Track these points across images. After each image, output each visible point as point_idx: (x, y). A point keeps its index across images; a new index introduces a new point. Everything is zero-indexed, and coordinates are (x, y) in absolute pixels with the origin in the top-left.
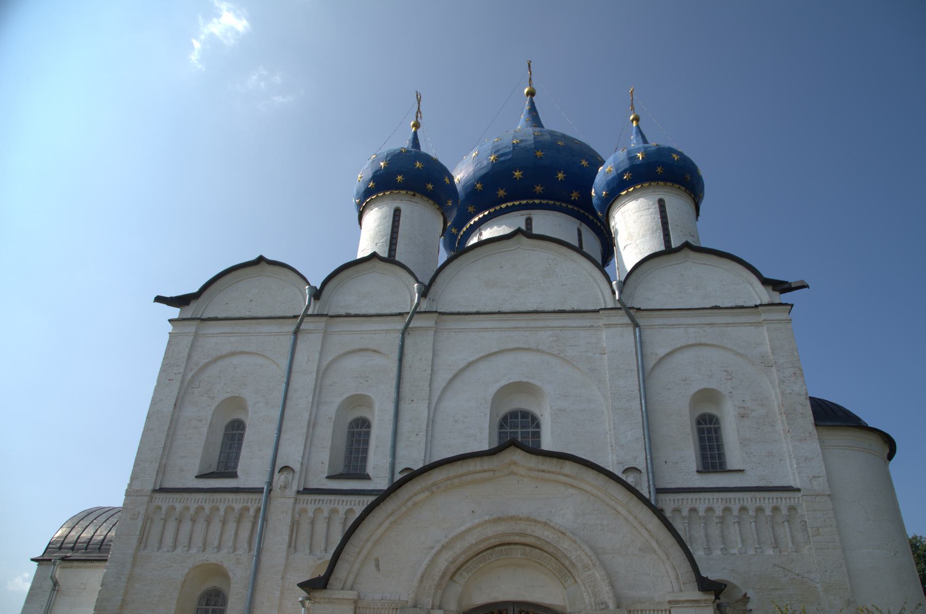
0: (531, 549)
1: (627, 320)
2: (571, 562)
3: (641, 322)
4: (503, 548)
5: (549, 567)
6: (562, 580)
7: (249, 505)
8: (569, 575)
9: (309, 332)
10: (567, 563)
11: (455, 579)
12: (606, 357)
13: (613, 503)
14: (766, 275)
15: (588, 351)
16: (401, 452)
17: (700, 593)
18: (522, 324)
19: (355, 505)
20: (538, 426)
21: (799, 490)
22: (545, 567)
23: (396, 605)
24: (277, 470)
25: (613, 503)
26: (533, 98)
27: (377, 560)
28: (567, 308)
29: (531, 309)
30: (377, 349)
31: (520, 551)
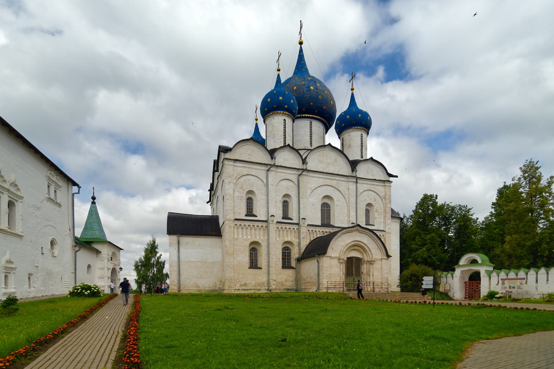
1: (355, 181)
3: (358, 181)
7: (263, 225)
10: (365, 250)
14: (389, 172)
15: (344, 188)
16: (301, 213)
18: (329, 177)
20: (330, 208)
24: (270, 216)
27: (332, 248)
28: (340, 174)
29: (331, 172)
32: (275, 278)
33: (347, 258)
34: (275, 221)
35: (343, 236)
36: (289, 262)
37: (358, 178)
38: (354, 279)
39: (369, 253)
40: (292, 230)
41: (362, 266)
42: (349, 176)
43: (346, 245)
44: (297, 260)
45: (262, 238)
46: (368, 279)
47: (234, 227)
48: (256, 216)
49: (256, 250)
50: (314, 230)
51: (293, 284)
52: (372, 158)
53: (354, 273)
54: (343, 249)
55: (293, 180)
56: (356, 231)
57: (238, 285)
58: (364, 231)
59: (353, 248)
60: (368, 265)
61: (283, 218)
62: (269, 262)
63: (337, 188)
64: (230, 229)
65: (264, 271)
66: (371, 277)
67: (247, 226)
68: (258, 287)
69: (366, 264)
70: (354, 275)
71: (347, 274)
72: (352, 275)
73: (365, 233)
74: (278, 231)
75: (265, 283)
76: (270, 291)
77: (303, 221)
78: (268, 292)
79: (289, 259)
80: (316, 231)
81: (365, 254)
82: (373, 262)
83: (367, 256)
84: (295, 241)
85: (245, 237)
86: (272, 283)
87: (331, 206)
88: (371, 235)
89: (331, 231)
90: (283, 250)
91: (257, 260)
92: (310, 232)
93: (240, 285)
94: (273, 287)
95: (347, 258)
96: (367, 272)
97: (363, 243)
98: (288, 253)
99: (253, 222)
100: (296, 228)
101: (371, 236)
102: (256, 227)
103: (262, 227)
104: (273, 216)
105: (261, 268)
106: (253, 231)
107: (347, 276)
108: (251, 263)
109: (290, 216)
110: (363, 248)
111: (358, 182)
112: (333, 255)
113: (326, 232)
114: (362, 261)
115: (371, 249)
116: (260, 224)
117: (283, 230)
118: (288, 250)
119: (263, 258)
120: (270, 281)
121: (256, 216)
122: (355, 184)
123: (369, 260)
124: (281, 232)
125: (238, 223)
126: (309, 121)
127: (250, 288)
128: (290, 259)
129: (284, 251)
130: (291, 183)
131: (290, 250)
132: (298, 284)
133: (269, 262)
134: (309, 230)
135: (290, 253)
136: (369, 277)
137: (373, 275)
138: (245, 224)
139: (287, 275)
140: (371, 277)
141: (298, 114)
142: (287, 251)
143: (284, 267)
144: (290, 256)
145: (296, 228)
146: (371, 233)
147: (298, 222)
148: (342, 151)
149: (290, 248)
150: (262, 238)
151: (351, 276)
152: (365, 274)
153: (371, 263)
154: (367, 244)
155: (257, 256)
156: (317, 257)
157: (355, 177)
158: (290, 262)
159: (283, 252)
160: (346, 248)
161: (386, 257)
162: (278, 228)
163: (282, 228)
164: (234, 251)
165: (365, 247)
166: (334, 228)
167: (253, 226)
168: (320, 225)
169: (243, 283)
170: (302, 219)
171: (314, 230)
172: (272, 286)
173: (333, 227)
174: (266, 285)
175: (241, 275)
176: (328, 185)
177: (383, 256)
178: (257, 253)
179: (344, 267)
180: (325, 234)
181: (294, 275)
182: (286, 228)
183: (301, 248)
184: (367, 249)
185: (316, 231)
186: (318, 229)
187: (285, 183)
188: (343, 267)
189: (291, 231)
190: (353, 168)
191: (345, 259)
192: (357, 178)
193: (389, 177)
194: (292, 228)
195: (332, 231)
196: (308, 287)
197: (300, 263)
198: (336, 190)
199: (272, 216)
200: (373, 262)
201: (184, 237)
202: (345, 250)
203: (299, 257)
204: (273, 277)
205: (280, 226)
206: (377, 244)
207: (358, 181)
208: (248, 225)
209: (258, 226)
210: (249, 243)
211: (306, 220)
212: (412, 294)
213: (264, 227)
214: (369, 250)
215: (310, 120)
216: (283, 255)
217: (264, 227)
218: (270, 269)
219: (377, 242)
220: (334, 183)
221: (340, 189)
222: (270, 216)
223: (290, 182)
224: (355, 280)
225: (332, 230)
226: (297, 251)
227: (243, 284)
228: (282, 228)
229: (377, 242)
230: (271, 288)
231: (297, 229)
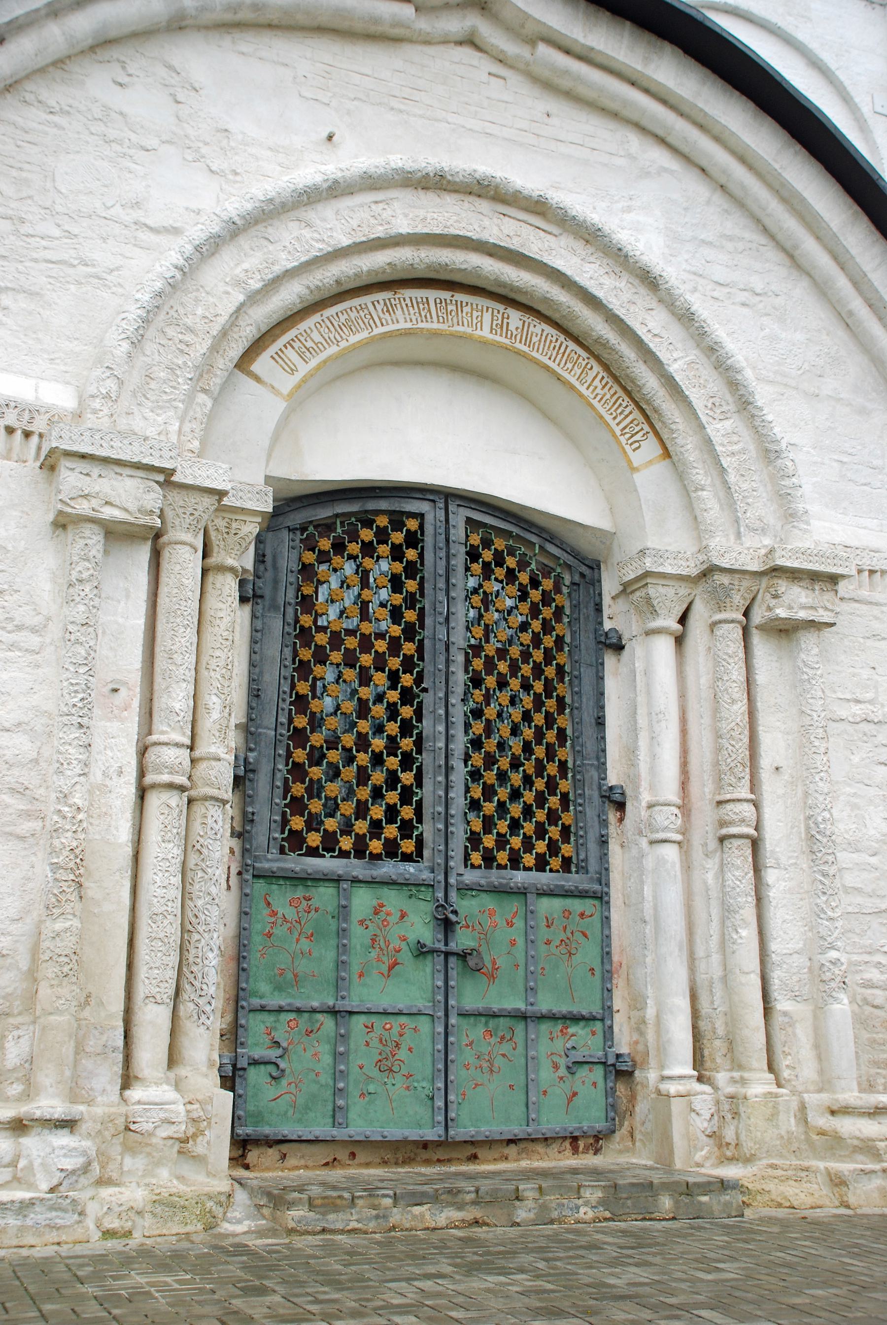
0: (529, 319)
4: (432, 294)
5: (583, 389)
6: (623, 439)
8: (647, 428)
10: (650, 383)
11: (257, 367)
13: (790, 225)
22: (572, 388)
23: (26, 416)
31: (487, 317)
41: (612, 686)
46: (727, 911)
66: (771, 876)
69: (679, 640)
83: (680, 474)
88: (743, 158)
114: (609, 586)
151: (391, 850)
214: (715, 385)
224: (463, 940)
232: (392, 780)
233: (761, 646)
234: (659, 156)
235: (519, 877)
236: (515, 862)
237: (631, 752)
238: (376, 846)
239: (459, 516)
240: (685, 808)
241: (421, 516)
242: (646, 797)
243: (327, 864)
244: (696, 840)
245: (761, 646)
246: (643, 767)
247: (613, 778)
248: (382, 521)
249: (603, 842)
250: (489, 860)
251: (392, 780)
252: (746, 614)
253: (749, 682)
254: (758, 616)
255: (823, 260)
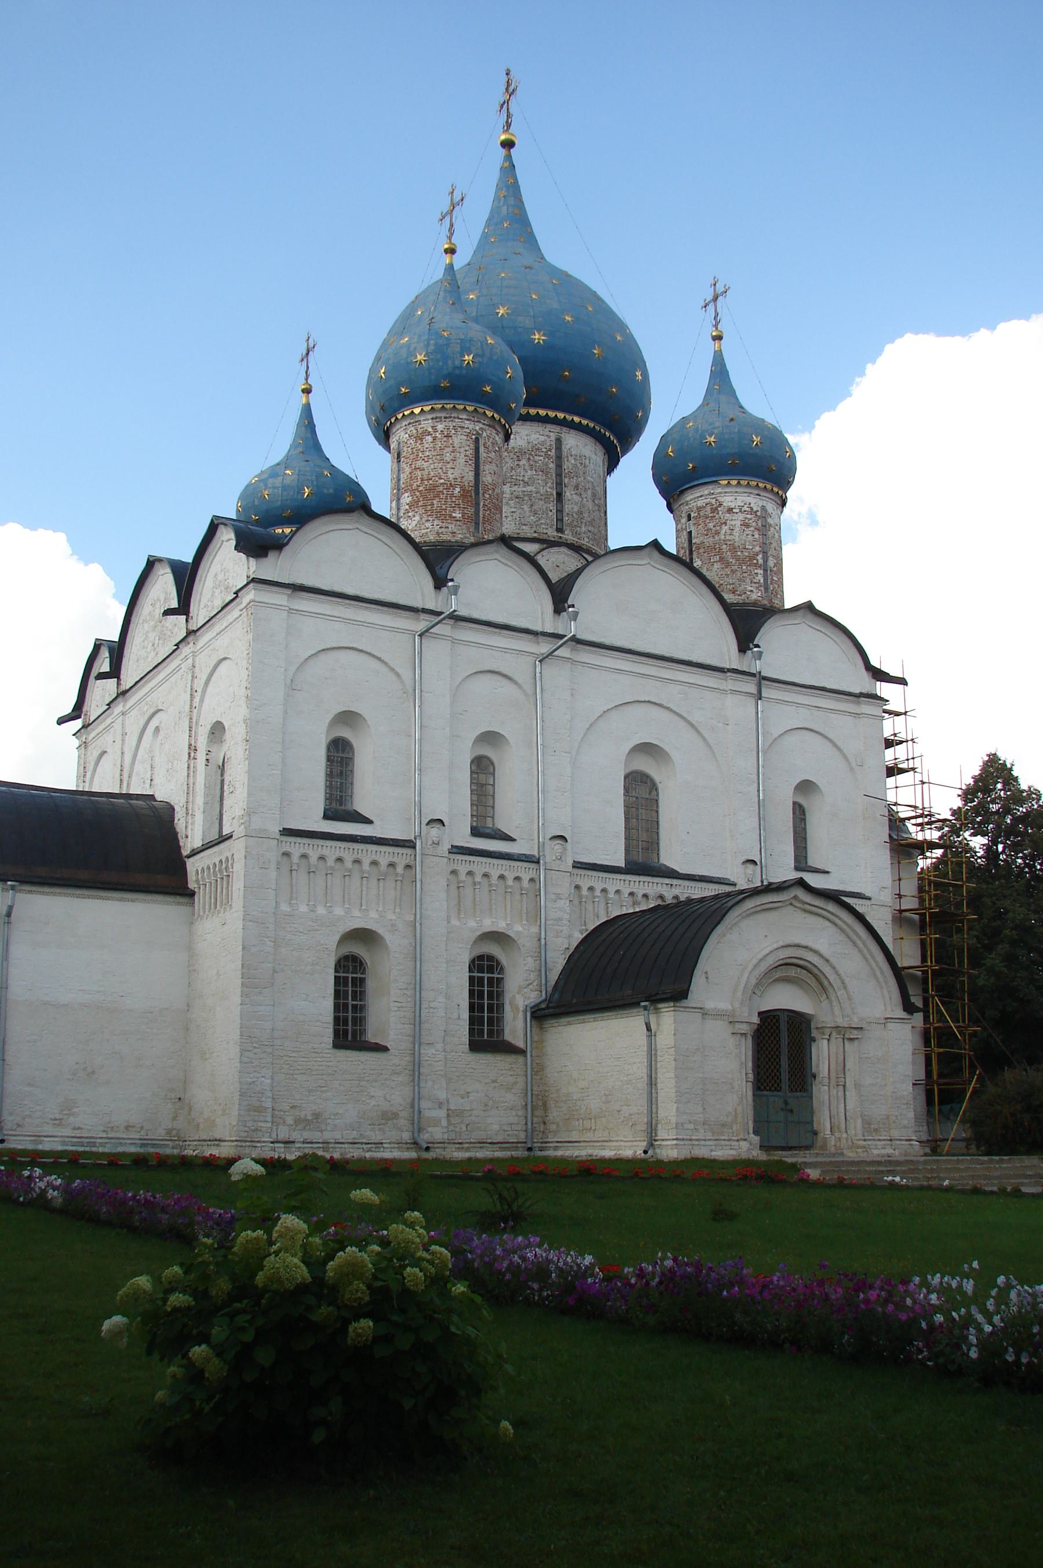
1: (752, 688)
2: (830, 982)
7: (395, 860)
9: (437, 637)
10: (826, 983)
12: (729, 728)
13: (855, 938)
14: (874, 662)
15: (712, 719)
17: (905, 1013)
19: (506, 870)
21: (870, 899)
25: (855, 938)
26: (511, 150)
27: (706, 972)
30: (510, 674)
32: (442, 1095)
33: (760, 1014)
34: (447, 846)
35: (744, 924)
36: (496, 1021)
37: (765, 678)
38: (786, 1103)
39: (841, 993)
40: (510, 882)
42: (729, 670)
43: (755, 961)
44: (532, 1013)
45: (391, 916)
47: (278, 863)
48: (368, 821)
49: (361, 963)
50: (599, 887)
51: (515, 1120)
52: (809, 607)
53: (785, 1076)
54: (746, 975)
55: (515, 678)
56: (791, 904)
57: (290, 1120)
58: (821, 905)
59: (778, 974)
60: (836, 1041)
61: (476, 832)
62: (417, 1022)
63: (684, 714)
64: (260, 871)
65: (396, 1061)
67: (331, 862)
68: (373, 1130)
69: (828, 1040)
70: (785, 1085)
71: (759, 1081)
72: (778, 1089)
73: (824, 912)
74: (453, 887)
75: (401, 1114)
76: (427, 1149)
77: (557, 845)
78: (413, 1155)
79: (496, 1007)
80: (604, 890)
81: (825, 1004)
82: (854, 1034)
83: (831, 1002)
84: (518, 929)
85: (321, 910)
86: (427, 1113)
87: (660, 786)
89: (666, 894)
90: (470, 971)
91: (362, 1008)
92: (580, 897)
93: (298, 1121)
94: (436, 1133)
95: (760, 1014)
96: (833, 1075)
97: (816, 952)
98: (491, 980)
99: (356, 846)
100: (526, 877)
101: (844, 926)
102: (366, 866)
103: (391, 869)
104: (441, 822)
105: (381, 1048)
106: (355, 882)
107: (759, 1089)
108: (337, 1020)
109: (503, 825)
110: (815, 976)
111: (763, 695)
112: (710, 1005)
113: (645, 896)
114: (813, 1025)
115: (847, 981)
116: (384, 855)
117: (475, 884)
118: (491, 969)
119: (392, 1004)
120: (424, 1104)
121: (368, 821)
122: (752, 701)
123: (841, 1022)
124: (468, 892)
125: (297, 847)
126: (553, 436)
127: (338, 1136)
128: (501, 1007)
129: (476, 974)
130: (506, 689)
131: (502, 970)
132: (535, 1119)
133: (417, 1022)
134: (577, 887)
135: (500, 980)
136: (841, 1094)
137: (857, 1086)
138: (326, 852)
139: (487, 1081)
140: (851, 1094)
141: (528, 403)
142: (486, 975)
143: (476, 1045)
144: (500, 994)
145: (526, 877)
146: (831, 907)
147: (536, 853)
148: (688, 560)
149: (498, 963)
150: (391, 916)
152: (826, 1081)
153: (849, 1034)
154: (832, 960)
155: (363, 993)
156: (645, 1008)
157: (753, 675)
158: (500, 1020)
159: (471, 979)
160: (757, 973)
161: (901, 1014)
162: (454, 872)
163: (470, 873)
164: (275, 971)
165: (826, 970)
166: (675, 882)
167: (357, 862)
168: (623, 866)
169: (307, 1113)
170: (551, 839)
171: (599, 887)
172: (430, 1129)
173: (672, 874)
174: (402, 1122)
175: (299, 1077)
176: (649, 702)
177: (889, 1009)
178: (362, 981)
179: (750, 1053)
180: (644, 907)
181: (521, 1080)
182: (502, 877)
183: (550, 965)
184: (832, 977)
185: (604, 890)
186: (614, 883)
187: (484, 686)
188: (746, 1048)
189: (506, 887)
190: (745, 641)
191: (756, 1020)
192: (762, 679)
193: (874, 680)
194: (495, 874)
195: (669, 896)
196: (589, 1136)
197: (541, 1028)
198: (682, 723)
199: (431, 822)
200: (854, 1034)
201: (30, 892)
202: (753, 981)
203: (540, 1003)
204: (436, 1088)
205: (464, 864)
206: (866, 959)
207: (763, 690)
208: (334, 857)
209: (374, 863)
210: (337, 938)
211: (569, 845)
212: (1001, 1161)
213: (400, 869)
214: (839, 981)
215: (556, 428)
216: (471, 993)
217: (400, 869)
218: (422, 1051)
219: (869, 950)
220: (670, 695)
221: (695, 717)
222: (425, 821)
223: (505, 682)
224: (789, 1107)
225: (671, 891)
226: (533, 976)
227: (309, 1117)
228: (470, 873)
229: (869, 950)
230: (424, 1138)
231: (532, 880)
232: (775, 1075)
233: (846, 1042)
234: (827, 923)
235: (799, 1094)
236: (796, 1091)
237: (818, 1066)
238: (773, 1089)
239: (786, 1013)
240: (829, 1078)
241: (779, 1016)
242: (821, 1076)
243: (765, 1093)
244: (832, 1085)
245: (846, 1042)
246: (821, 1068)
247: (814, 1070)
248: (772, 1017)
249: (812, 1085)
250: (792, 1090)
251: (775, 1075)
252: (844, 1035)
253: (844, 1052)
254: (847, 1036)
255: (861, 946)
